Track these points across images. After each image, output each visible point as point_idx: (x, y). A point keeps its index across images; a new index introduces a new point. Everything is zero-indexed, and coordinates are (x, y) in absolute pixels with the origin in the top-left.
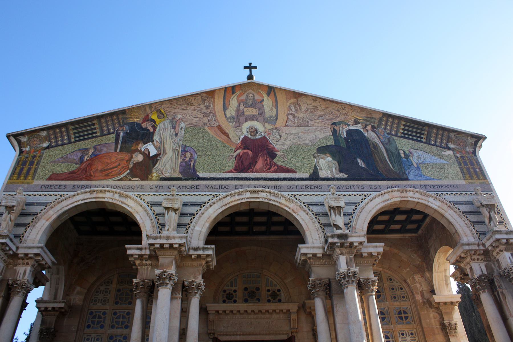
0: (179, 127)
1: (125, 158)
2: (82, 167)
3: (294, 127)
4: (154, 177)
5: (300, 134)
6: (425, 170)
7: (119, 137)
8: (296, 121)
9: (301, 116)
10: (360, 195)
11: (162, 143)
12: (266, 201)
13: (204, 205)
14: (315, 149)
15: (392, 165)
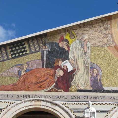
1: (51, 73)
2: (20, 80)
4: (73, 89)
7: (44, 54)
11: (76, 61)
13: (110, 112)
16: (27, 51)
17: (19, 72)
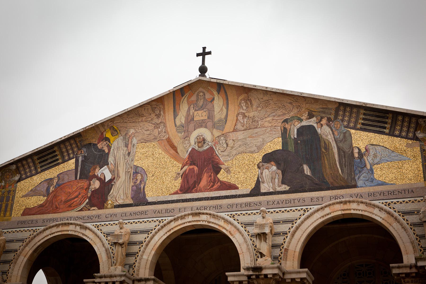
0: (131, 144)
1: (84, 186)
2: (48, 200)
4: (109, 205)
5: (248, 139)
6: (379, 173)
8: (245, 123)
9: (251, 114)
10: (299, 211)
11: (116, 165)
12: (206, 223)
14: (261, 157)
15: (341, 169)
16: (58, 160)
17: (47, 188)
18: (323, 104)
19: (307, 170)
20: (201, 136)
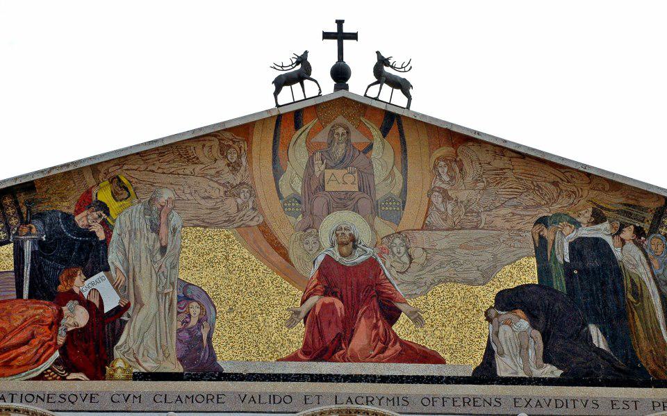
0: (167, 225)
3: (444, 230)
4: (119, 371)
8: (450, 212)
9: (464, 195)
11: (131, 274)
18: (630, 197)
19: (598, 336)
20: (345, 229)
